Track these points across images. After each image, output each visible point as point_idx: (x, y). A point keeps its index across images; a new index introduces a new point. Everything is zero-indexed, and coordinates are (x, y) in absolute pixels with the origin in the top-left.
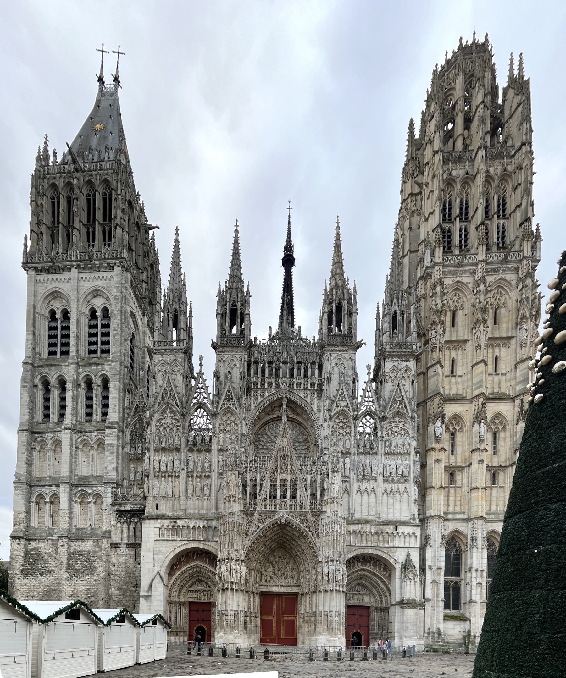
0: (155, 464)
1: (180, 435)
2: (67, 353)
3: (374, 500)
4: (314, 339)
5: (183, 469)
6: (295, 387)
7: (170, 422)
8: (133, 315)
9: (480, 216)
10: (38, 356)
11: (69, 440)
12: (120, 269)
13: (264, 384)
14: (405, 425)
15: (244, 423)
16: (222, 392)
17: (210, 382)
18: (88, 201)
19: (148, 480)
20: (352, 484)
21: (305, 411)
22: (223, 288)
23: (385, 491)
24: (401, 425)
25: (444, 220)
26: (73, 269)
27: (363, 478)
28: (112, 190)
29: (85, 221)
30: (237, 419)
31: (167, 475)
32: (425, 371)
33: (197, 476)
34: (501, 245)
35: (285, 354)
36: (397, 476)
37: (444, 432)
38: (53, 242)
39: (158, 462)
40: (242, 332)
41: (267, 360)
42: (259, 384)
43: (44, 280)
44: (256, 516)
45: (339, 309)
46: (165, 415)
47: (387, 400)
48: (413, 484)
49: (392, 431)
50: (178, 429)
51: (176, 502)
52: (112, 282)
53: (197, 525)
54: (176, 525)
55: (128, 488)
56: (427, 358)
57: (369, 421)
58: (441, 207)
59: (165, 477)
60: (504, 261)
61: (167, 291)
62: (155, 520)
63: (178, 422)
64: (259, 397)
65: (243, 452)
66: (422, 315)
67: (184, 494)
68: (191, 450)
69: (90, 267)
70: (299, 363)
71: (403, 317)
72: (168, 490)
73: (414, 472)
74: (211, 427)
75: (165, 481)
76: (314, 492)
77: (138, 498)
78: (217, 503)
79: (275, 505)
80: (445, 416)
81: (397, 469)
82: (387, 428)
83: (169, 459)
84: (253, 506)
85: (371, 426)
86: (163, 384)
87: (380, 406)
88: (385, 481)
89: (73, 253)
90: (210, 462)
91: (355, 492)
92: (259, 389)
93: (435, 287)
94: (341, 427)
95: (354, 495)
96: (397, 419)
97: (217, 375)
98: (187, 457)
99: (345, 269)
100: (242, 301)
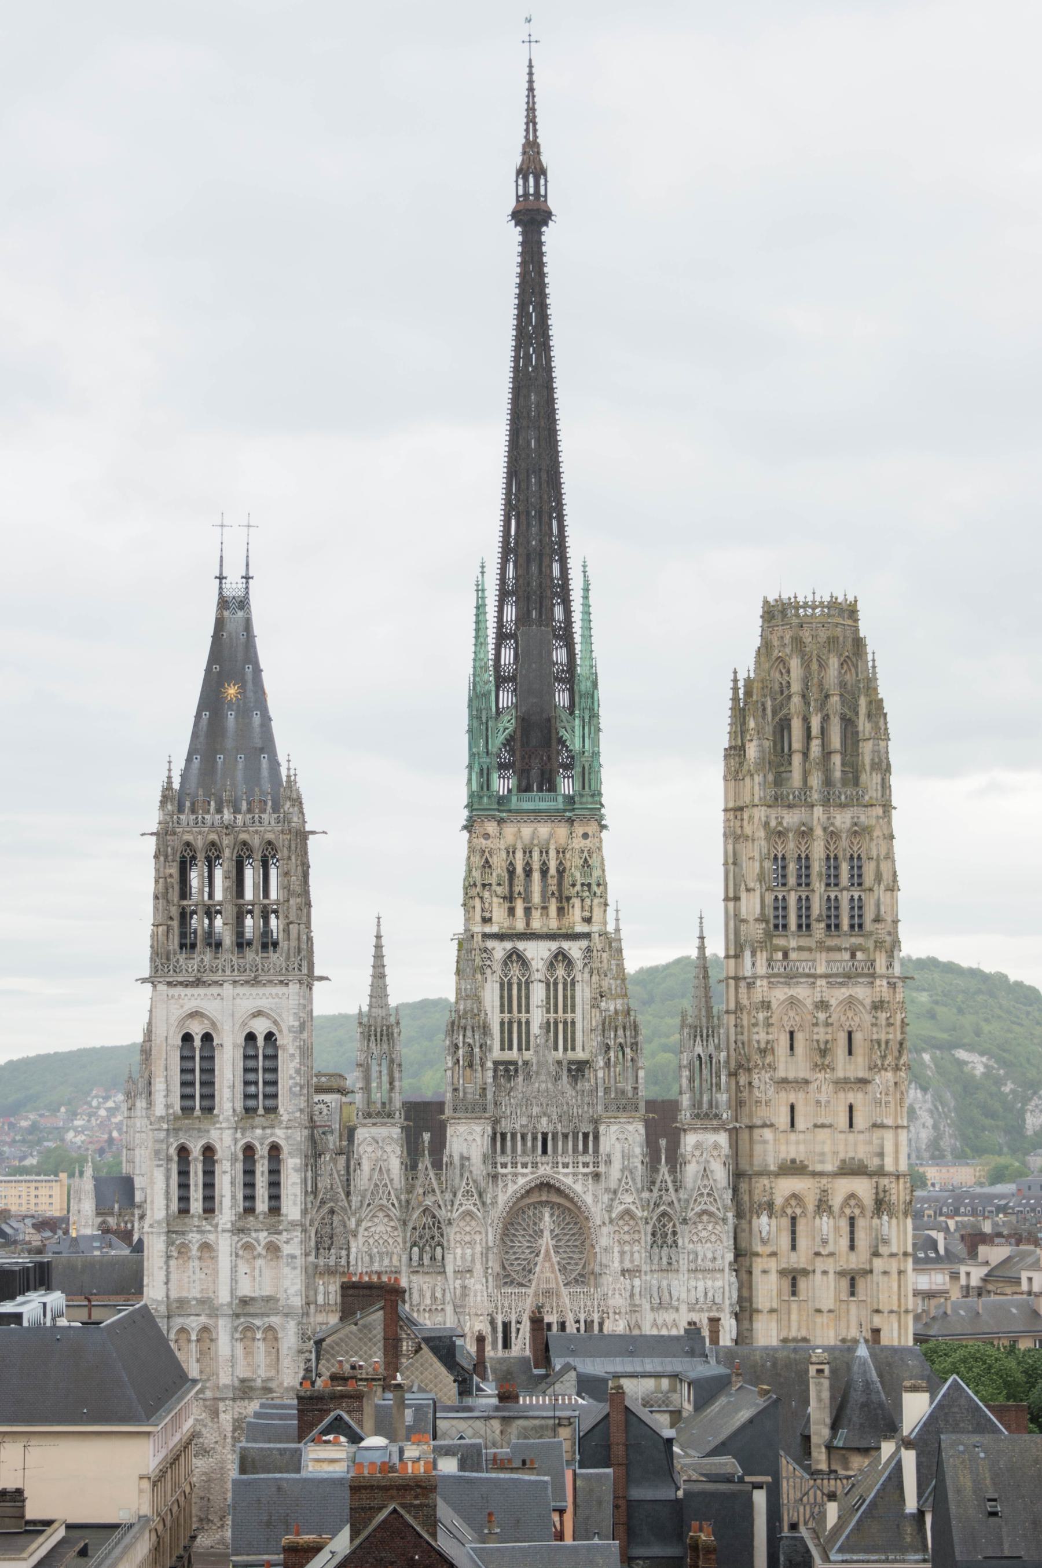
7: (383, 1229)
12: (298, 986)
26: (225, 984)
43: (180, 995)
46: (376, 1220)
48: (728, 1316)
63: (396, 1229)
64: (510, 1184)
73: (730, 1298)
81: (706, 1293)
88: (691, 1309)
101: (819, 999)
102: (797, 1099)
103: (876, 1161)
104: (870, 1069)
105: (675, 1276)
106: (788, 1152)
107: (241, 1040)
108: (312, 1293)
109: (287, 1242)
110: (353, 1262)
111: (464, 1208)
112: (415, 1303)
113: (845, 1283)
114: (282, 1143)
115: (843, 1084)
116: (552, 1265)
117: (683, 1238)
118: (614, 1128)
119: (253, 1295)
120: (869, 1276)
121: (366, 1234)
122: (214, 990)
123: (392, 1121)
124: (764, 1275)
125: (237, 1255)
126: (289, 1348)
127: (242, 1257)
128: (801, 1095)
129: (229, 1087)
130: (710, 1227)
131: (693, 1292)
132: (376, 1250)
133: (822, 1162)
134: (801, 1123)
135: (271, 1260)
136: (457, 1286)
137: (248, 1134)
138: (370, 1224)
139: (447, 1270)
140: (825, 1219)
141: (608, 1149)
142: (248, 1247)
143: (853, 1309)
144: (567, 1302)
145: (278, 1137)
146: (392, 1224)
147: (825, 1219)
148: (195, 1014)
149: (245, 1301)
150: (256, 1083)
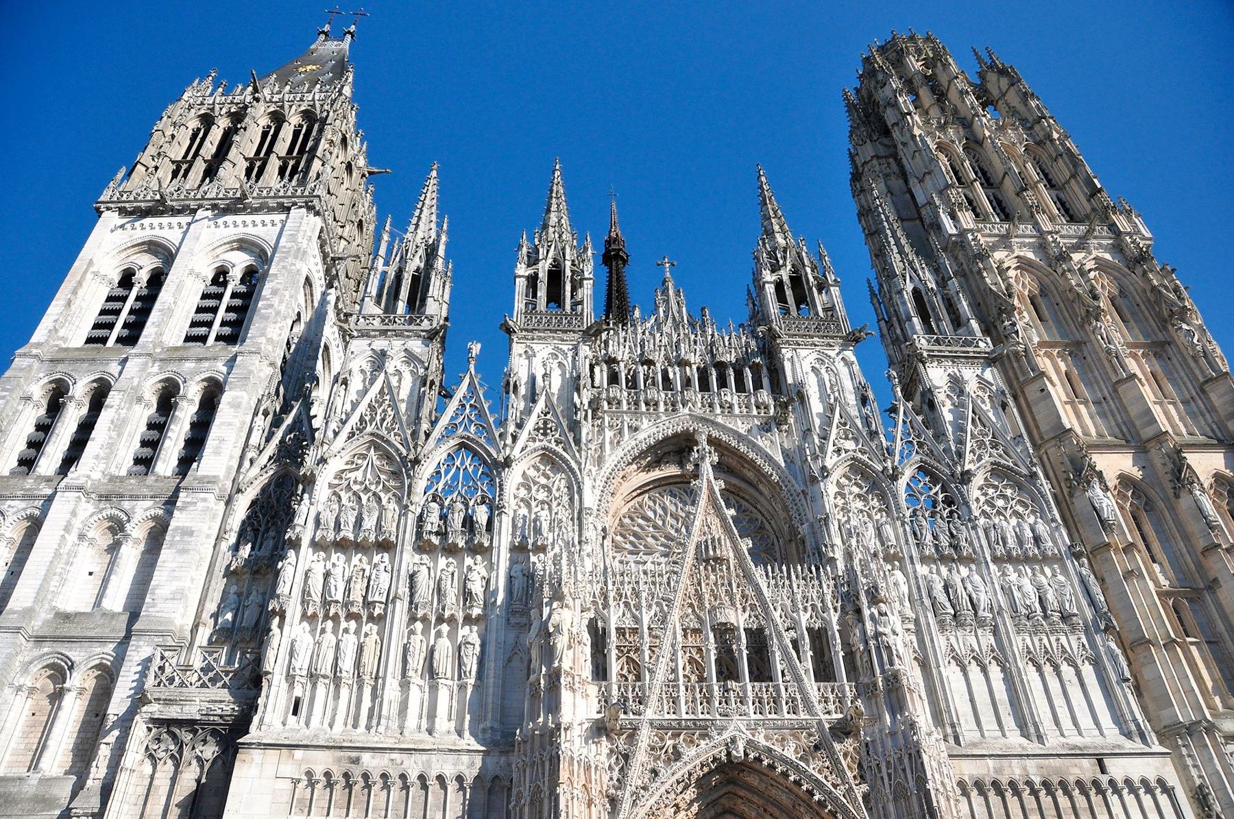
6: (718, 410)
12: (304, 210)
19: (281, 626)
24: (1009, 492)
26: (199, 212)
44: (646, 736)
46: (360, 462)
49: (993, 506)
53: (433, 773)
54: (357, 772)
59: (336, 618)
62: (285, 751)
73: (1092, 603)
78: (503, 698)
82: (977, 500)
89: (211, 189)
92: (626, 412)
95: (942, 669)
105: (973, 567)
109: (182, 509)
118: (803, 352)
121: (336, 482)
122: (184, 220)
123: (416, 328)
125: (82, 537)
131: (1017, 594)
136: (519, 573)
138: (348, 467)
139: (495, 544)
147: (1198, 493)
149: (66, 617)
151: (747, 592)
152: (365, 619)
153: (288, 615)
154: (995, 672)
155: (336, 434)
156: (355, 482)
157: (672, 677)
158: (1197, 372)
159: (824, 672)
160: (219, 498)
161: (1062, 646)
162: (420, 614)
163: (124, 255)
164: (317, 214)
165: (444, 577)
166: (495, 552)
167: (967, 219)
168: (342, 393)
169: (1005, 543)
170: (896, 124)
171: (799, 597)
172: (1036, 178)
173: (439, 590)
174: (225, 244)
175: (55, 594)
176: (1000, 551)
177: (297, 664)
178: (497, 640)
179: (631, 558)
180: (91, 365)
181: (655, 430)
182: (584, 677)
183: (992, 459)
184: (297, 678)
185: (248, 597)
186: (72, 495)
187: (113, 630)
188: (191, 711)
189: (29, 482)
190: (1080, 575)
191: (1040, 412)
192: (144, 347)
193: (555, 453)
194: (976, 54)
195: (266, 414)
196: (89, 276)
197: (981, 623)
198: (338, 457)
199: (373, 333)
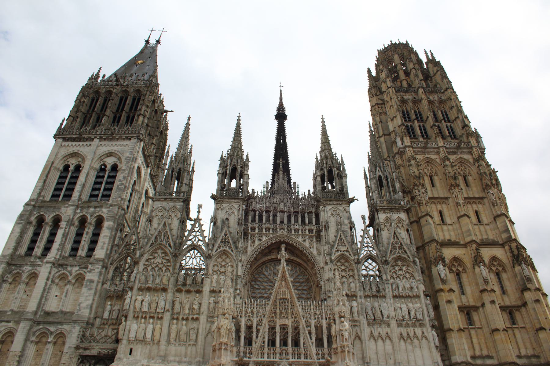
0: (136, 304)
1: (169, 274)
2: (70, 196)
3: (390, 347)
4: (309, 194)
5: (168, 311)
7: (160, 262)
8: (139, 168)
9: (431, 121)
10: (41, 198)
11: (47, 274)
12: (136, 140)
13: (262, 229)
14: (409, 268)
15: (240, 265)
16: (218, 236)
17: (207, 227)
18: (121, 100)
19: (126, 321)
20: (362, 329)
21: (305, 254)
22: (225, 153)
23: (401, 336)
25: (406, 121)
26: (95, 140)
27: (373, 322)
28: (141, 95)
29: (115, 111)
30: (233, 261)
31: (148, 316)
32: (417, 219)
33: (183, 319)
34: (453, 137)
35: (282, 205)
36: (411, 320)
37: (448, 274)
38: (84, 122)
39: (140, 302)
40: (239, 186)
41: (264, 209)
42: (257, 229)
45: (330, 173)
46: (156, 255)
47: (386, 246)
48: (430, 329)
49: (396, 274)
50: (168, 269)
51: (155, 347)
52: (127, 148)
55: (99, 328)
56: (416, 209)
57: (371, 265)
58: (401, 115)
59: (145, 318)
60: (458, 147)
61: (174, 155)
64: (257, 241)
65: (238, 294)
66: (404, 177)
67: (166, 338)
68: (179, 291)
69: (111, 139)
70: (294, 212)
71: (387, 180)
72: (147, 333)
73: (429, 316)
74: (203, 267)
75: (145, 323)
76: (320, 337)
77: (109, 340)
78: (204, 349)
79: (275, 354)
80: (445, 260)
81: (409, 313)
82: (390, 271)
83: (154, 299)
84: (248, 355)
85: (374, 269)
86: (158, 226)
87: (380, 251)
88: (399, 325)
89: (99, 130)
90: (200, 304)
91: (367, 338)
92: (257, 233)
93: (409, 161)
94: (344, 270)
95: (367, 342)
96: (399, 263)
97: (214, 220)
98: (174, 297)
99: (332, 146)
100: (241, 164)
101: (443, 157)
102: (442, 207)
103: (504, 236)
104: (484, 189)
105: (384, 300)
106: (444, 235)
107: (97, 166)
108: (100, 310)
109: (90, 272)
110: (132, 279)
111: (221, 249)
112: (175, 312)
113: (506, 316)
114: (105, 216)
115: (469, 200)
116: (287, 284)
117: (386, 273)
118: (329, 208)
119: (56, 311)
120: (523, 309)
121: (147, 263)
122: (88, 143)
124: (449, 305)
125: (53, 281)
126: (69, 347)
127: (57, 285)
128: (444, 206)
129: (81, 185)
130: (404, 268)
132: (151, 273)
133: (470, 235)
134: (448, 220)
135: (78, 287)
137: (85, 210)
138: (151, 257)
139: (204, 289)
140: (482, 267)
141: (326, 218)
142: (63, 277)
143: (517, 332)
144: (300, 310)
145: (103, 213)
146: (167, 258)
147: (482, 267)
148: (74, 155)
149: (48, 314)
150: (99, 189)
151: (294, 312)
152: (156, 318)
153: (128, 317)
154: (388, 341)
155: (147, 243)
156: (154, 263)
157: (263, 344)
158: (493, 211)
159: (319, 342)
160: (103, 267)
161: (415, 332)
162: (175, 317)
163: (65, 159)
164: (141, 141)
165: (185, 302)
166: (204, 293)
167: (407, 141)
168: (149, 225)
169: (399, 289)
170: (385, 91)
171: (312, 314)
172: (442, 118)
173: (183, 307)
174: (105, 154)
175: (44, 305)
176: (396, 293)
177: (131, 336)
178: (203, 328)
179: (257, 291)
180: (54, 209)
181: (268, 241)
182: (232, 344)
183: (398, 255)
184: (131, 341)
185: (114, 306)
186: (49, 265)
187: (65, 319)
188: (94, 352)
189: (32, 259)
190: (426, 303)
191: (425, 230)
192: (74, 201)
193: (228, 252)
194: (425, 51)
195: (121, 231)
196: (52, 168)
197: (384, 323)
198: (147, 254)
199: (162, 200)
